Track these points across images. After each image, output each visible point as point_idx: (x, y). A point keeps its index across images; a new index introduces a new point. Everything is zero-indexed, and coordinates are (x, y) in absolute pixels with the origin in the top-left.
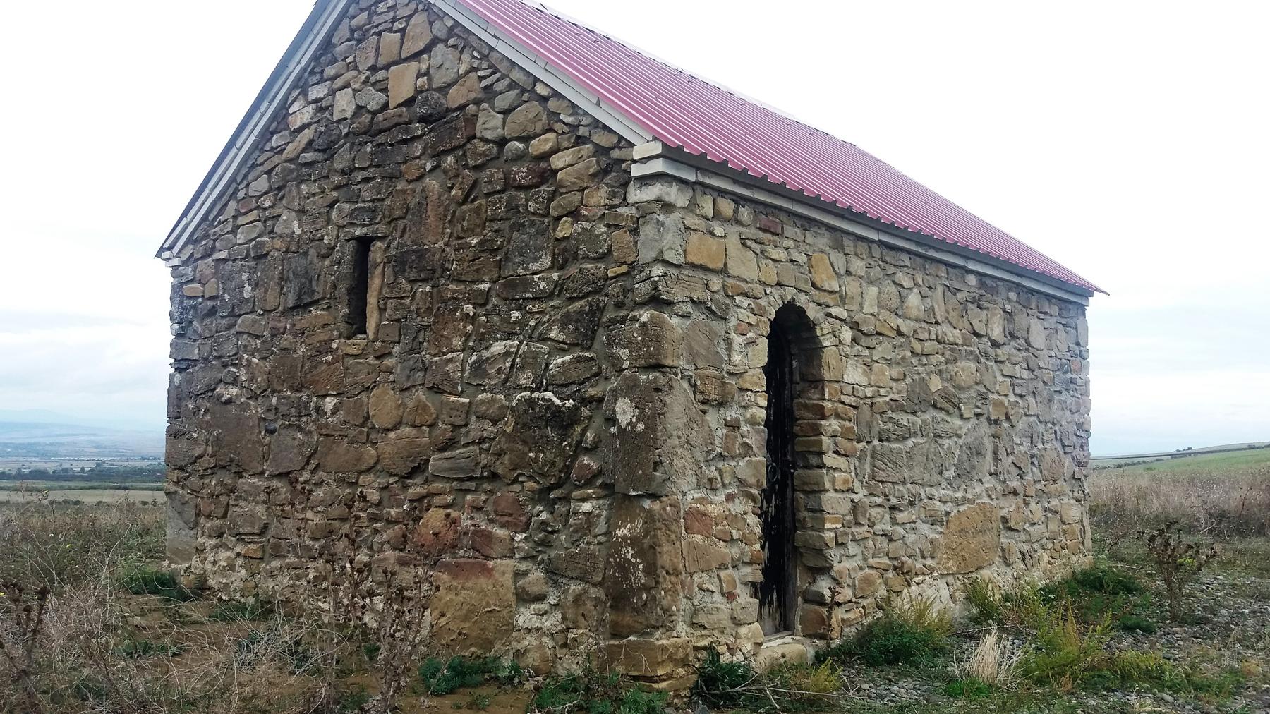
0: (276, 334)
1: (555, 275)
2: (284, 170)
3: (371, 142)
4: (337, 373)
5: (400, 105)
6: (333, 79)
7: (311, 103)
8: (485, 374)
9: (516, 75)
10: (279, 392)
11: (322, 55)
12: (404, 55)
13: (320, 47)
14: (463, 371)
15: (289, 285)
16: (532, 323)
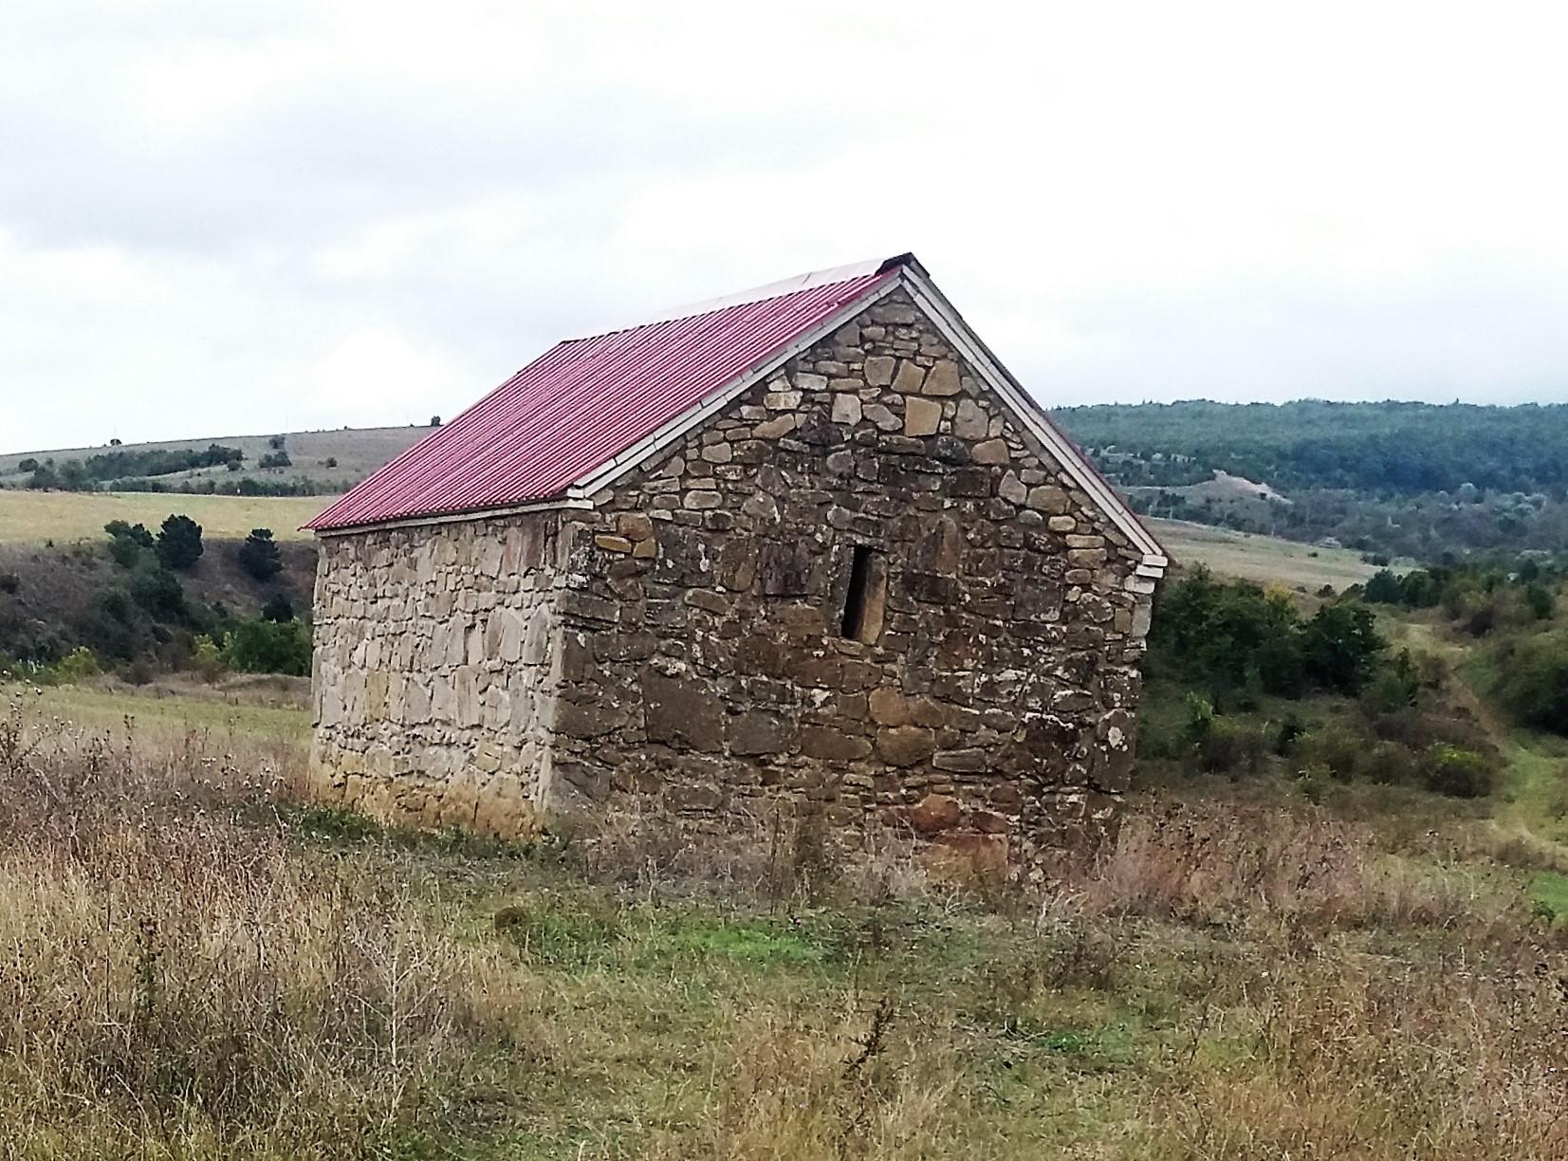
0: (743, 615)
1: (1064, 628)
2: (760, 448)
5: (917, 437)
6: (831, 376)
7: (799, 389)
8: (996, 693)
9: (1046, 460)
15: (769, 571)
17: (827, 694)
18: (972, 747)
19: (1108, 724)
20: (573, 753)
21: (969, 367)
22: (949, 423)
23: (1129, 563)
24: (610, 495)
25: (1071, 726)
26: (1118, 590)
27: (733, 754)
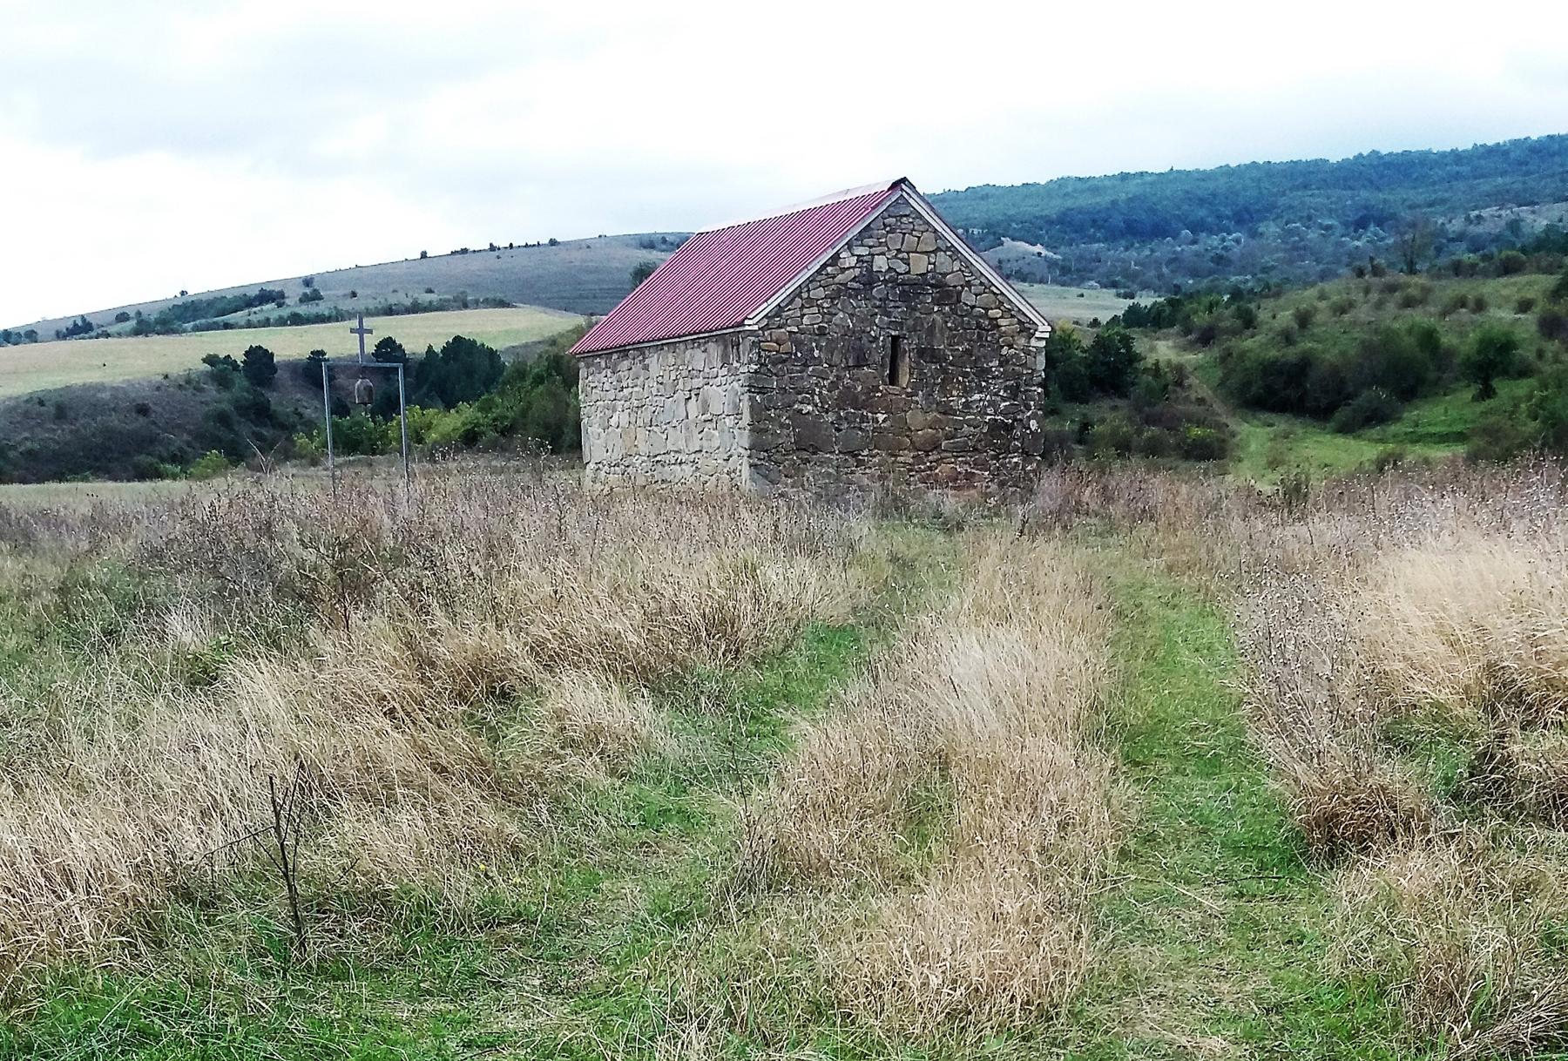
0: (838, 377)
6: (870, 247)
9: (983, 280)
20: (759, 459)
27: (840, 452)
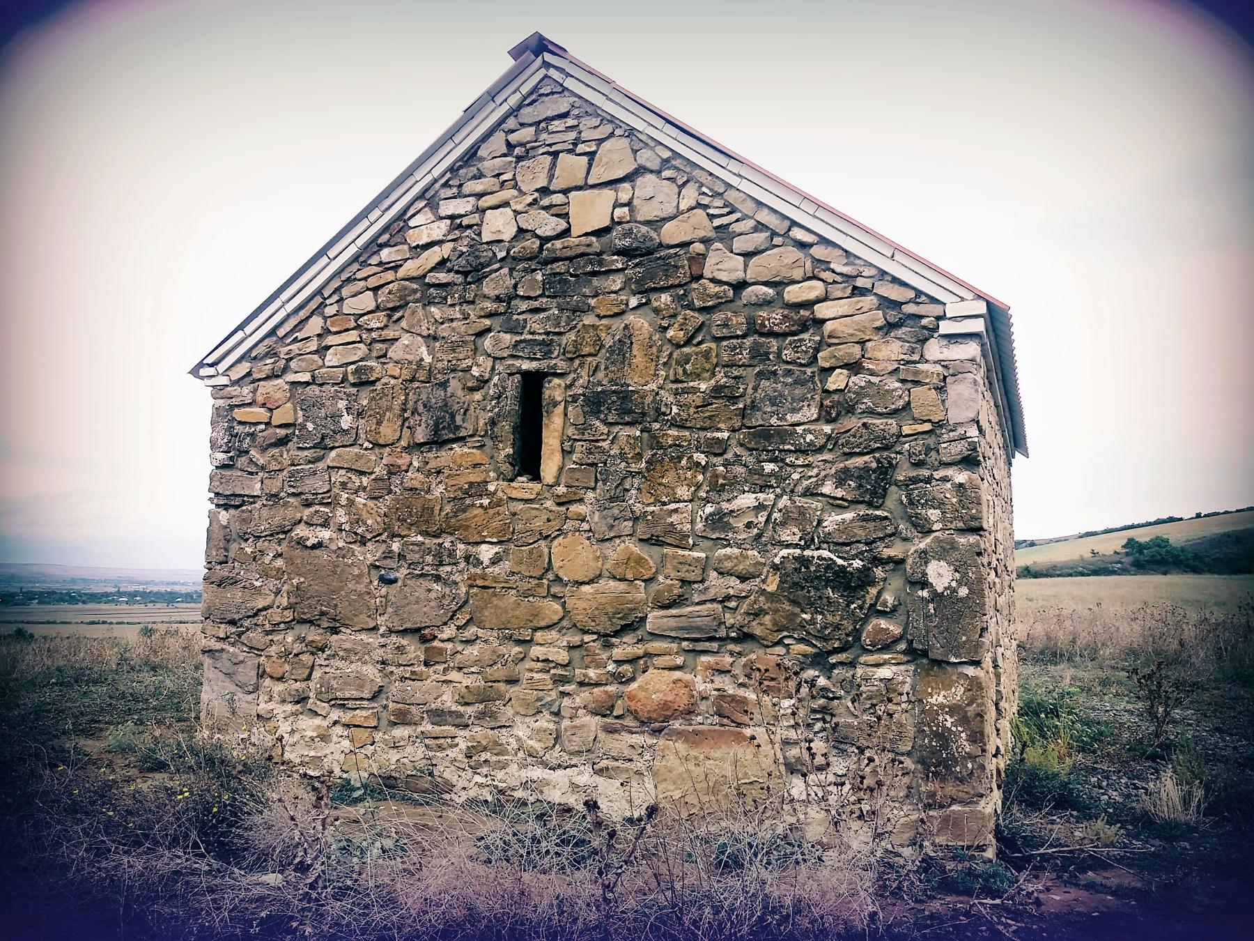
0: (393, 470)
1: (827, 429)
3: (541, 270)
4: (500, 518)
5: (586, 234)
6: (480, 196)
7: (444, 218)
8: (728, 527)
10: (403, 537)
11: (461, 167)
12: (590, 182)
13: (461, 159)
14: (692, 522)
15: (417, 417)
16: (796, 476)
17: (497, 549)
18: (704, 602)
19: (924, 556)
21: (641, 137)
22: (626, 209)
23: (924, 322)
24: (244, 368)
25: (857, 564)
26: (908, 362)
